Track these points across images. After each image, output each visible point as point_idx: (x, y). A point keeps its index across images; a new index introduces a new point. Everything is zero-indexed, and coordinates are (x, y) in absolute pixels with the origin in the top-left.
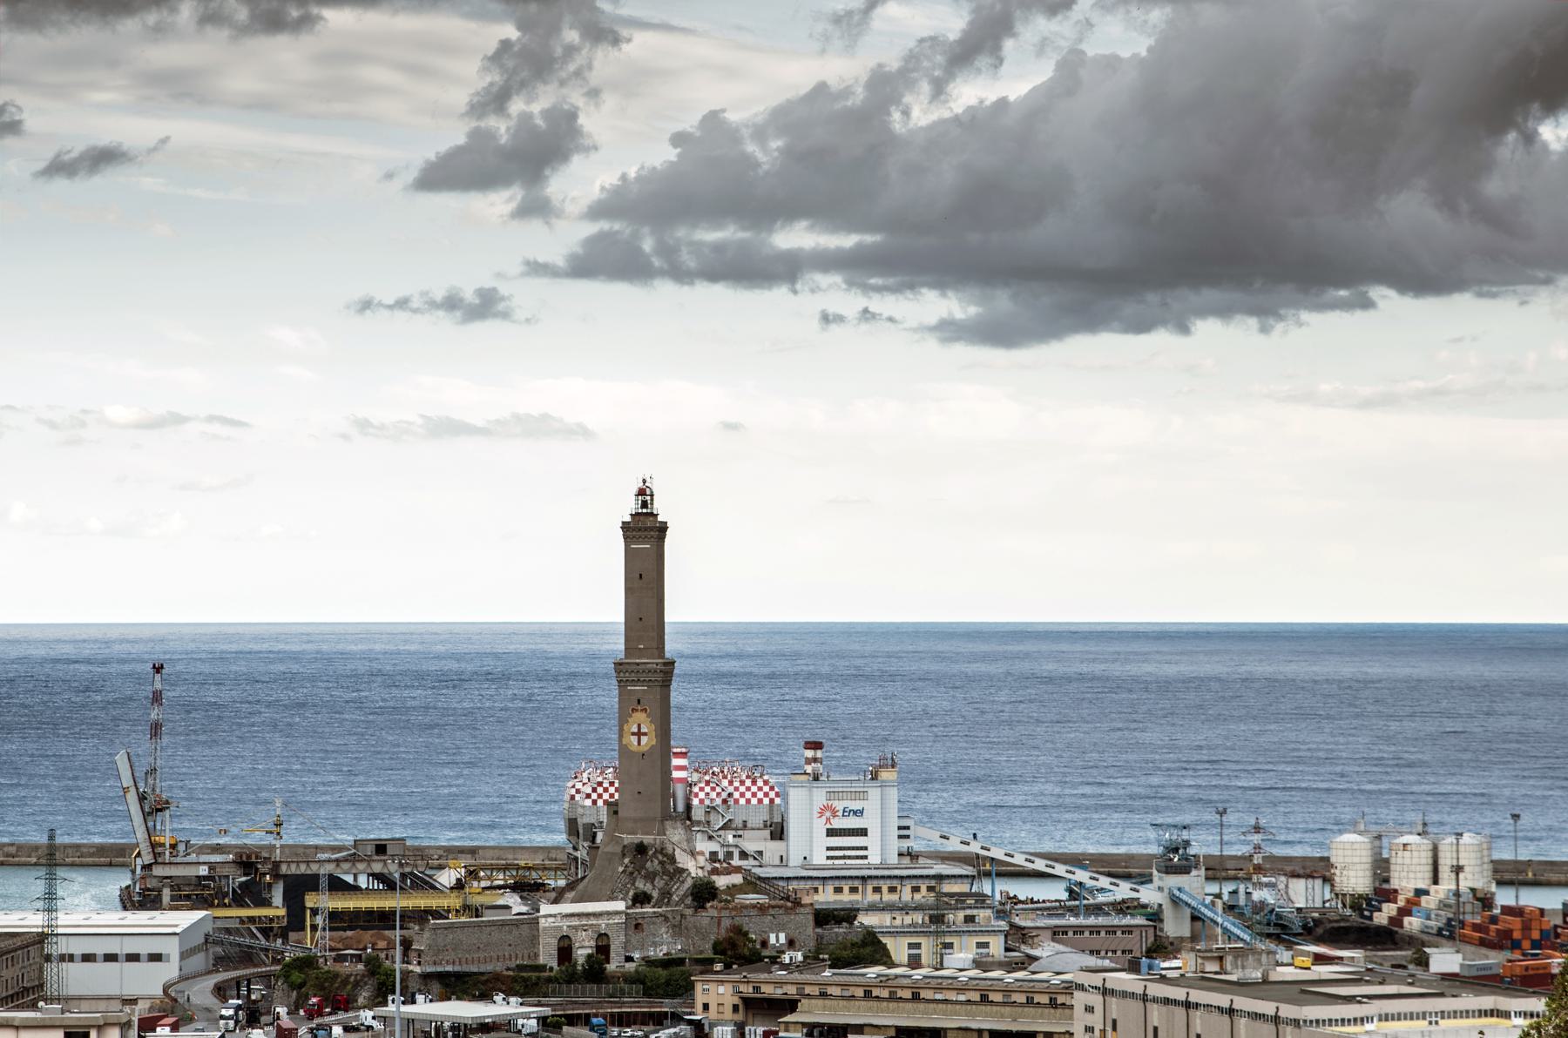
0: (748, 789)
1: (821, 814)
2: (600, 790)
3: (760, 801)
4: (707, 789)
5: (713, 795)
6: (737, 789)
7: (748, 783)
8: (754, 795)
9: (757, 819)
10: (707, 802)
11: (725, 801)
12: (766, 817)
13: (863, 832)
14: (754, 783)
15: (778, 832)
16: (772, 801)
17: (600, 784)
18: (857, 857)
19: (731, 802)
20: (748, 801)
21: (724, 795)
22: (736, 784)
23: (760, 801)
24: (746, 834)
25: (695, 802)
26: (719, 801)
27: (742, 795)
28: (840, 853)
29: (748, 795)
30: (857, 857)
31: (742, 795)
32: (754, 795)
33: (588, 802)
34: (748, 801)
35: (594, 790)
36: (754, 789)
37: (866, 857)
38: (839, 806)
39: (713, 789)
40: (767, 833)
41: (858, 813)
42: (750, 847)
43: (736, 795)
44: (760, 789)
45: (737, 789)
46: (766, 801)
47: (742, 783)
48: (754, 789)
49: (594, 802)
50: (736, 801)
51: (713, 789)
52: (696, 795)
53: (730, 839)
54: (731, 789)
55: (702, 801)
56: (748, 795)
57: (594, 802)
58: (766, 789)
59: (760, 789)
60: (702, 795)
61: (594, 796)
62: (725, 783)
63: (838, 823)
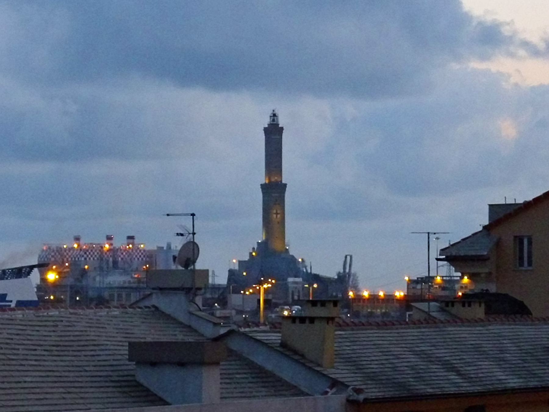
2: (88, 253)
3: (142, 259)
5: (126, 256)
8: (140, 256)
11: (131, 259)
21: (130, 257)
26: (128, 259)
27: (136, 256)
31: (136, 256)
32: (140, 256)
33: (83, 259)
49: (85, 259)
51: (126, 254)
55: (122, 259)
57: (85, 259)
60: (122, 256)
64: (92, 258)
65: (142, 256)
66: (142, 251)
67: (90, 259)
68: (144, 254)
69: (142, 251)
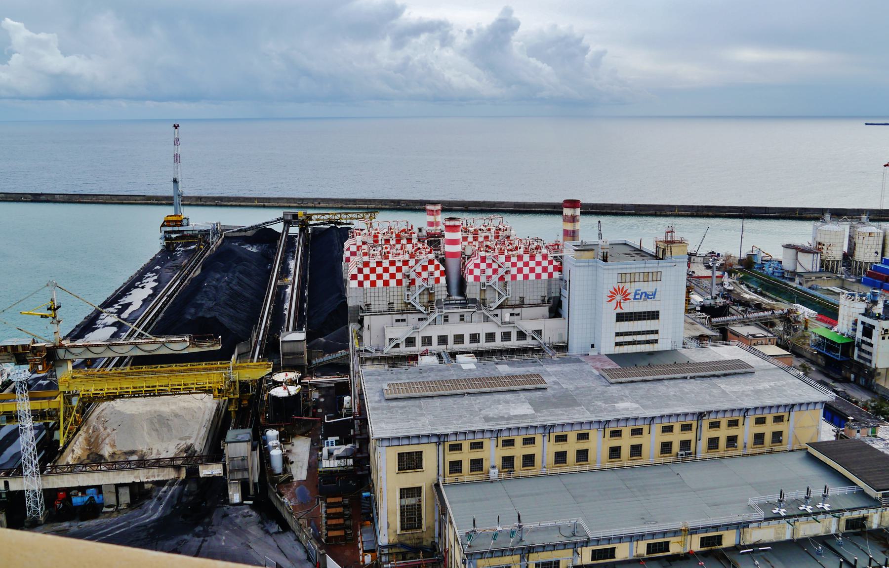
0: (526, 264)
1: (611, 298)
2: (366, 271)
3: (538, 276)
4: (483, 266)
5: (489, 272)
7: (526, 258)
8: (532, 270)
9: (533, 296)
10: (483, 279)
11: (502, 278)
12: (544, 293)
13: (654, 315)
14: (532, 257)
15: (556, 309)
16: (550, 275)
17: (366, 264)
18: (648, 342)
19: (508, 278)
20: (526, 277)
21: (501, 272)
22: (514, 259)
23: (538, 276)
24: (525, 312)
25: (470, 279)
26: (495, 278)
27: (520, 271)
29: (526, 270)
30: (648, 342)
32: (532, 270)
34: (526, 277)
35: (360, 271)
36: (532, 264)
37: (656, 341)
38: (631, 288)
39: (489, 266)
40: (545, 310)
42: (528, 327)
44: (538, 264)
45: (514, 265)
46: (545, 276)
47: (520, 258)
48: (532, 264)
49: (361, 284)
50: (514, 277)
51: (489, 266)
52: (471, 272)
53: (507, 318)
55: (477, 278)
57: (361, 284)
58: (545, 263)
59: (538, 264)
60: (477, 272)
61: (360, 277)
62: (502, 258)
63: (629, 307)
64: (380, 283)
67: (373, 284)
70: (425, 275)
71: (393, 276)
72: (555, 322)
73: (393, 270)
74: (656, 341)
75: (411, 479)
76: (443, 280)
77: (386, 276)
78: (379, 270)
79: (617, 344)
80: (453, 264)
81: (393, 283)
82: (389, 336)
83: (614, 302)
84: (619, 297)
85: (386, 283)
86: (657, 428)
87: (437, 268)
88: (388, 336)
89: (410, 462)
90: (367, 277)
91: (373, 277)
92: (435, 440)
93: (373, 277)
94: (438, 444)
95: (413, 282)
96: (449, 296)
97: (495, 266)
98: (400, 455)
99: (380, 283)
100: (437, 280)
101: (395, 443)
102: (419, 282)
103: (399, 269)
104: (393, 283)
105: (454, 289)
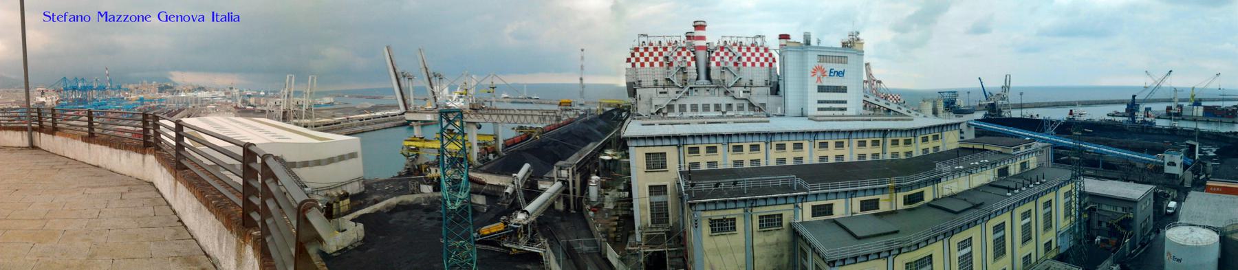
1: (814, 73)
2: (637, 55)
3: (762, 65)
4: (722, 54)
5: (727, 59)
6: (744, 54)
8: (758, 59)
10: (722, 64)
11: (736, 64)
12: (767, 78)
13: (843, 90)
19: (741, 65)
21: (735, 59)
23: (762, 65)
25: (713, 64)
26: (731, 64)
27: (749, 59)
28: (834, 106)
29: (753, 59)
31: (749, 59)
32: (758, 59)
33: (629, 65)
34: (753, 64)
36: (757, 55)
37: (845, 109)
39: (726, 54)
41: (840, 74)
43: (744, 59)
44: (762, 55)
46: (766, 64)
49: (634, 65)
50: (745, 64)
51: (726, 54)
54: (740, 54)
55: (718, 64)
56: (753, 59)
57: (634, 65)
60: (718, 59)
61: (633, 60)
63: (827, 82)
64: (647, 64)
65: (762, 60)
66: (762, 50)
67: (642, 65)
68: (766, 55)
69: (762, 50)
70: (679, 59)
71: (656, 59)
72: (773, 99)
73: (656, 54)
74: (845, 109)
75: (658, 178)
76: (693, 64)
77: (651, 59)
78: (646, 54)
79: (819, 109)
80: (702, 55)
81: (657, 64)
82: (655, 103)
83: (815, 78)
84: (819, 74)
85: (652, 64)
86: (855, 142)
87: (688, 54)
88: (655, 103)
89: (656, 162)
90: (638, 60)
91: (642, 60)
92: (675, 142)
93: (642, 60)
94: (679, 147)
95: (671, 64)
96: (698, 79)
97: (731, 54)
98: (648, 155)
99: (647, 64)
100: (689, 64)
101: (642, 143)
102: (675, 64)
103: (661, 54)
104: (657, 64)
105: (703, 75)
